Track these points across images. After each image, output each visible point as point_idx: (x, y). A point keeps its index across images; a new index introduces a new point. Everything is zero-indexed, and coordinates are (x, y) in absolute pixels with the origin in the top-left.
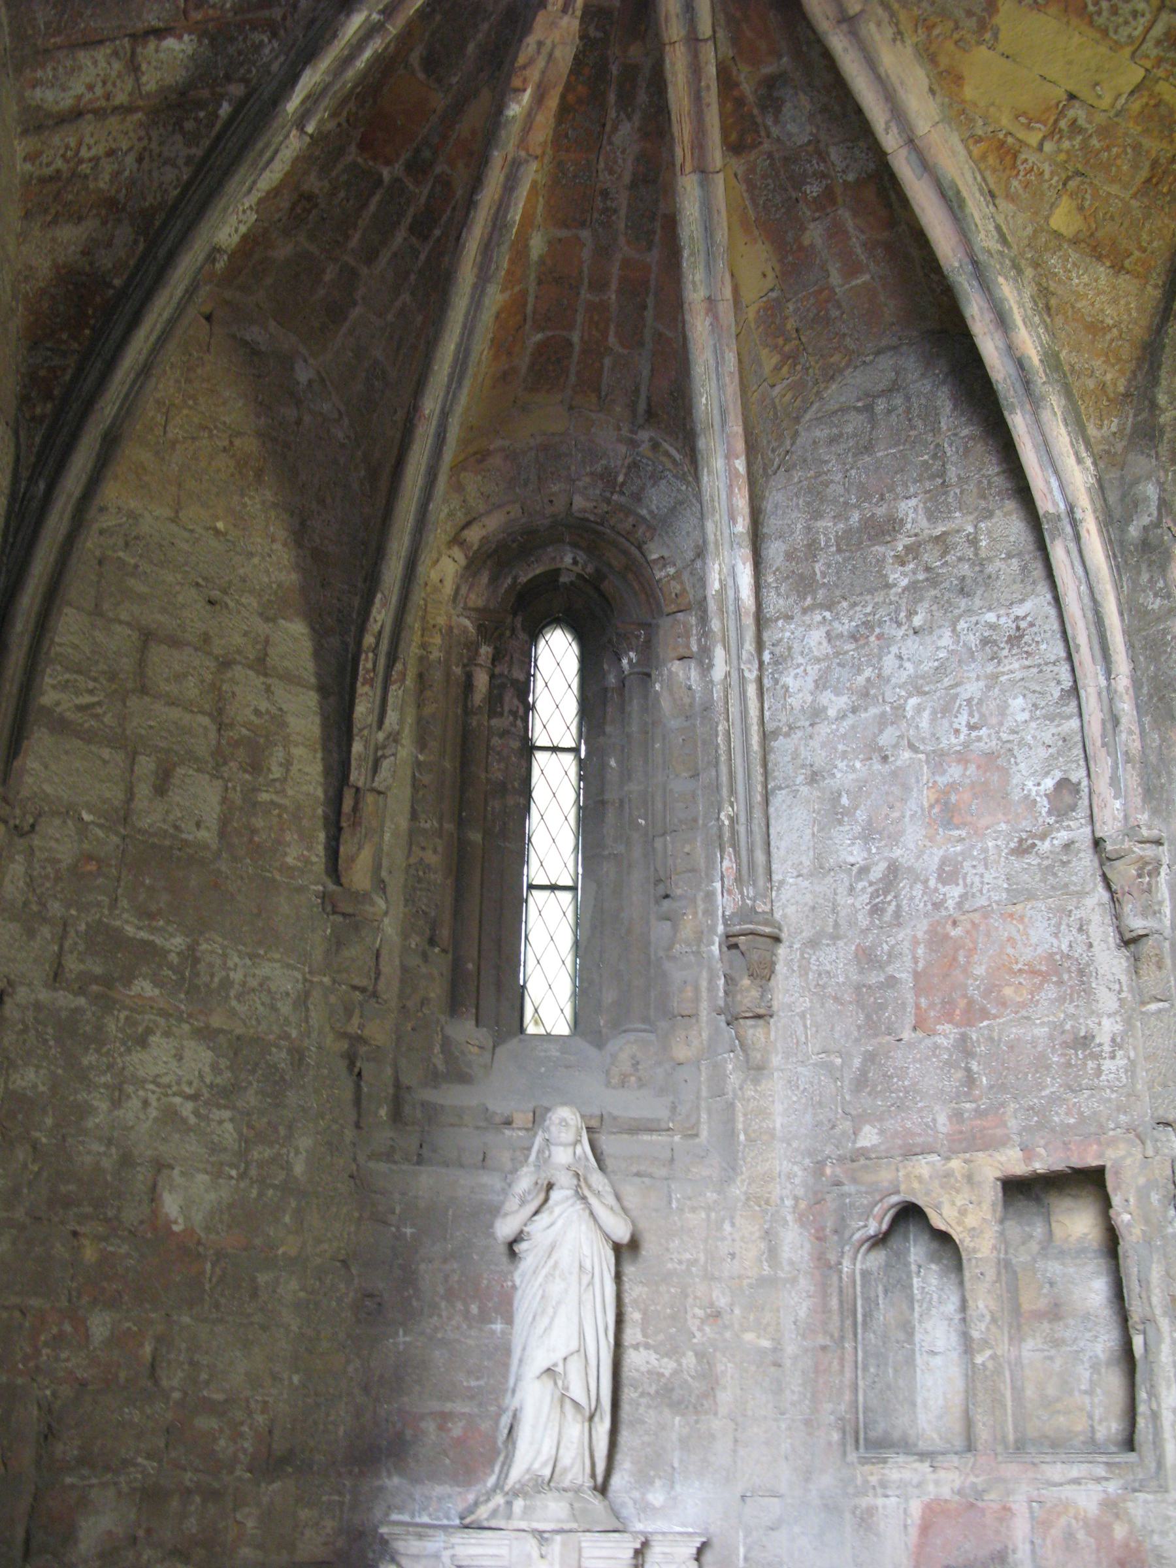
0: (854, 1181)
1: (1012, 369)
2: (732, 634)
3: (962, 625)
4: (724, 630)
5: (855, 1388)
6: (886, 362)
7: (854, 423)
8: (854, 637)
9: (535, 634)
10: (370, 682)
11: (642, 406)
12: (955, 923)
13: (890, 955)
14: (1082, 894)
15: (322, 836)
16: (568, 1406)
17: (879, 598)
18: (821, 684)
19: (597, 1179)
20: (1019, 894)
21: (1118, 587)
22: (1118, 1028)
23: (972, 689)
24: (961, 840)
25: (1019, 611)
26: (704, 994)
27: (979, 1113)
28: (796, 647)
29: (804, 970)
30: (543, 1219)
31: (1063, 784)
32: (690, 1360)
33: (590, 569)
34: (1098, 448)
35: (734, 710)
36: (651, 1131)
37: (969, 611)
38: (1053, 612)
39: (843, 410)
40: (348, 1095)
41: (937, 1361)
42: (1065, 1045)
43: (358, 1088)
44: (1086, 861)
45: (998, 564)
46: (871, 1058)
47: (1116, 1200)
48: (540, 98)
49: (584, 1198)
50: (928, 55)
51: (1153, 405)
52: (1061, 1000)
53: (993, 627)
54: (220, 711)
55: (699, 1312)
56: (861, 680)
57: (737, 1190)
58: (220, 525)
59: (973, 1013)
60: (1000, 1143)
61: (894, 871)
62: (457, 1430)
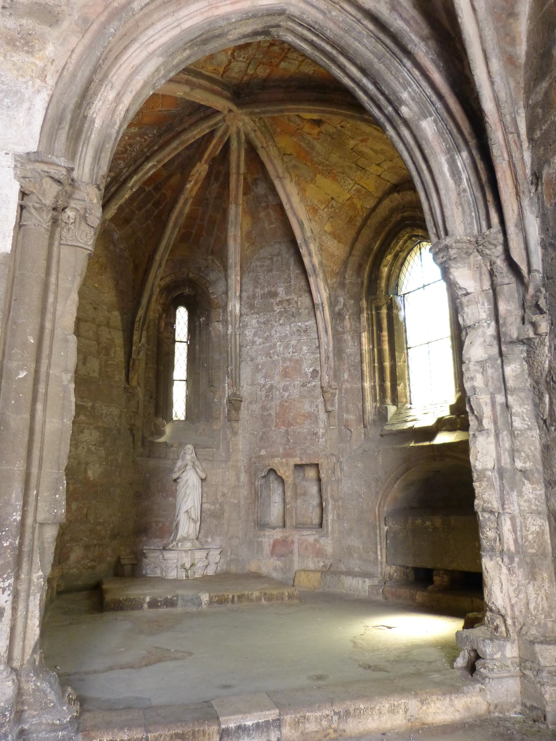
0: (259, 463)
1: (311, 267)
2: (233, 321)
3: (292, 325)
4: (231, 321)
5: (258, 513)
6: (277, 246)
7: (268, 262)
8: (264, 323)
9: (176, 308)
10: (138, 330)
11: (210, 250)
12: (286, 402)
13: (270, 408)
14: (317, 398)
15: (124, 372)
16: (191, 520)
17: (272, 313)
18: (255, 334)
19: (197, 463)
20: (302, 396)
21: (332, 323)
22: (324, 431)
23: (294, 342)
24: (288, 381)
25: (307, 324)
26: (222, 413)
27: (290, 449)
28: (249, 323)
29: (248, 409)
30: (185, 473)
31: (315, 370)
32: (218, 506)
33: (193, 293)
34: (330, 286)
35: (233, 341)
36: (208, 448)
37: (294, 322)
38: (315, 326)
39: (264, 258)
40: (131, 439)
41: (276, 504)
42: (311, 434)
43: (134, 438)
44: (319, 390)
45: (302, 310)
46: (264, 433)
47: (321, 472)
48: (196, 184)
49: (195, 468)
50: (298, 184)
51: (344, 278)
52: (311, 423)
53: (300, 327)
54: (98, 339)
55: (220, 494)
56: (265, 335)
57: (230, 463)
58: (96, 285)
59: (290, 424)
60: (294, 456)
61: (272, 387)
62: (160, 525)
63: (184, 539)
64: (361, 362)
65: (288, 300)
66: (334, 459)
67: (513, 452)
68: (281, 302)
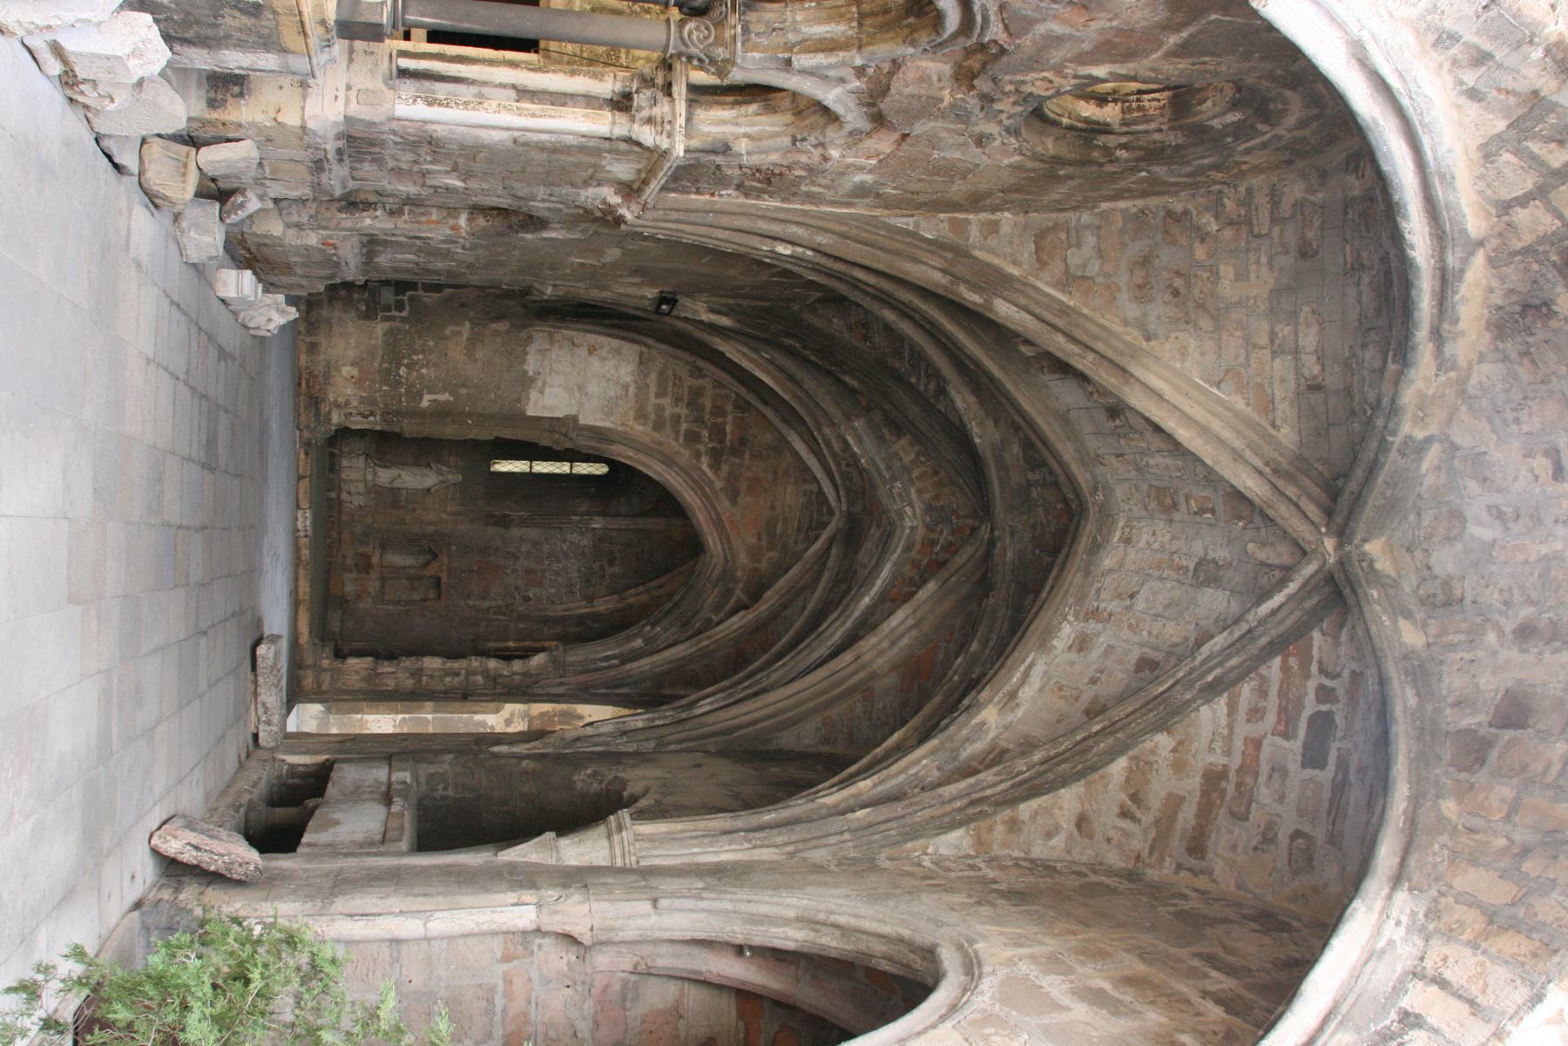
18: (572, 543)
23: (560, 580)
61: (518, 558)
63: (375, 473)
64: (534, 640)
65: (604, 576)
66: (443, 613)
67: (431, 676)
68: (603, 569)
